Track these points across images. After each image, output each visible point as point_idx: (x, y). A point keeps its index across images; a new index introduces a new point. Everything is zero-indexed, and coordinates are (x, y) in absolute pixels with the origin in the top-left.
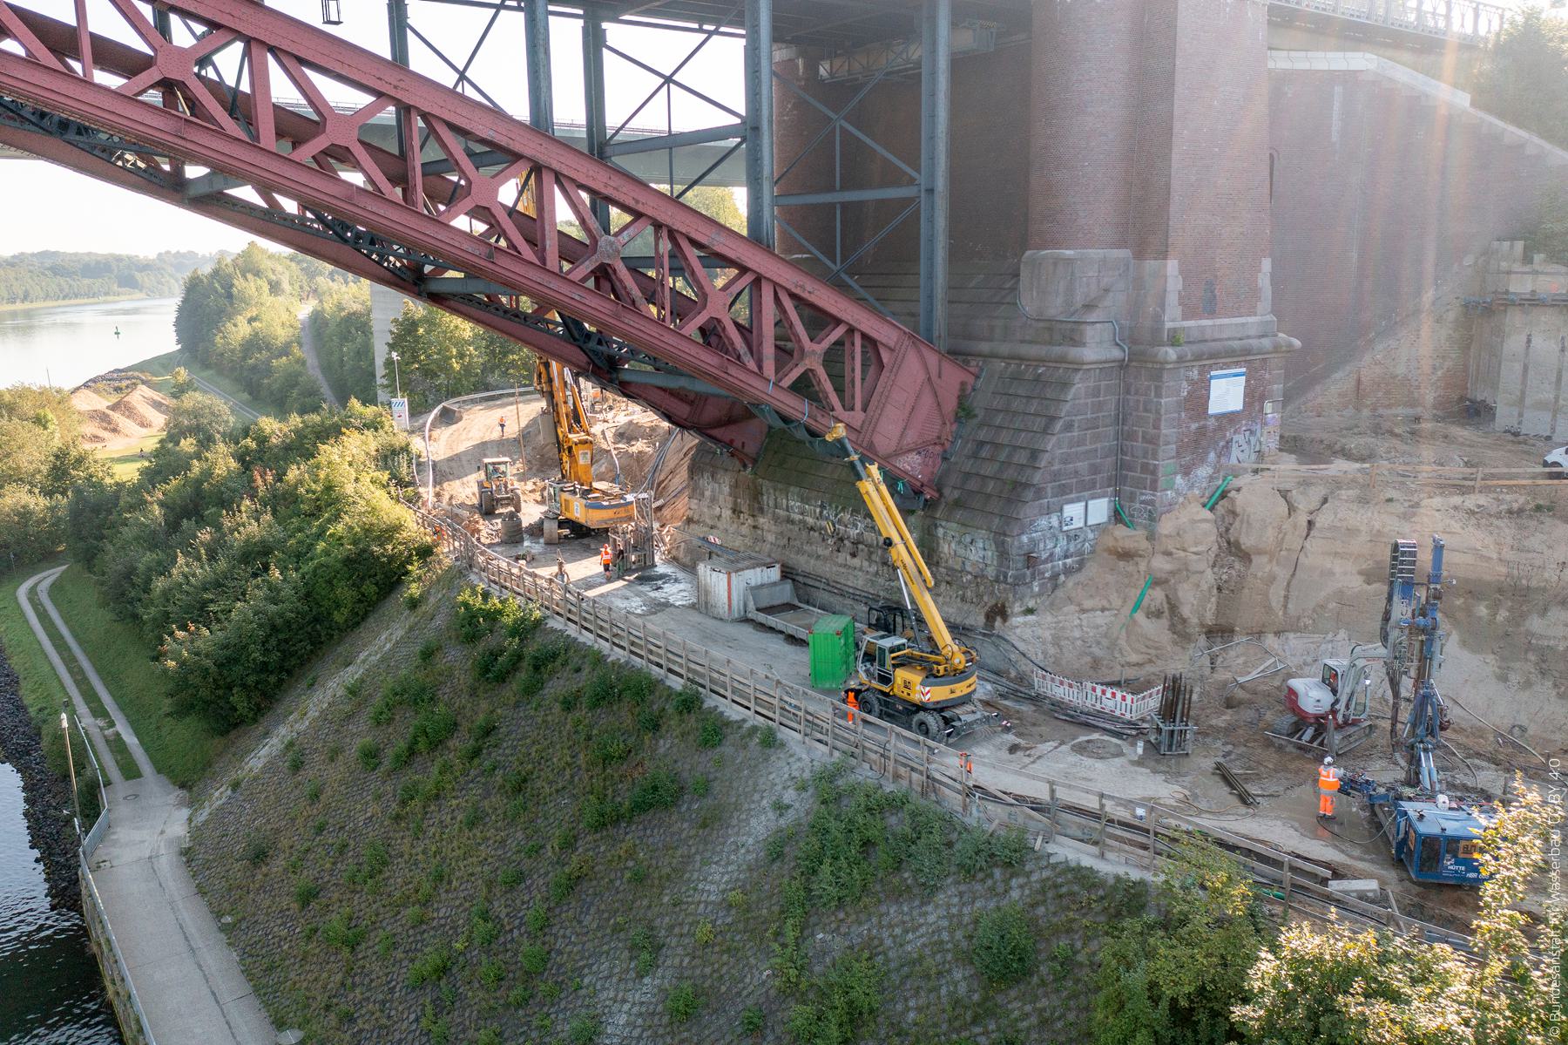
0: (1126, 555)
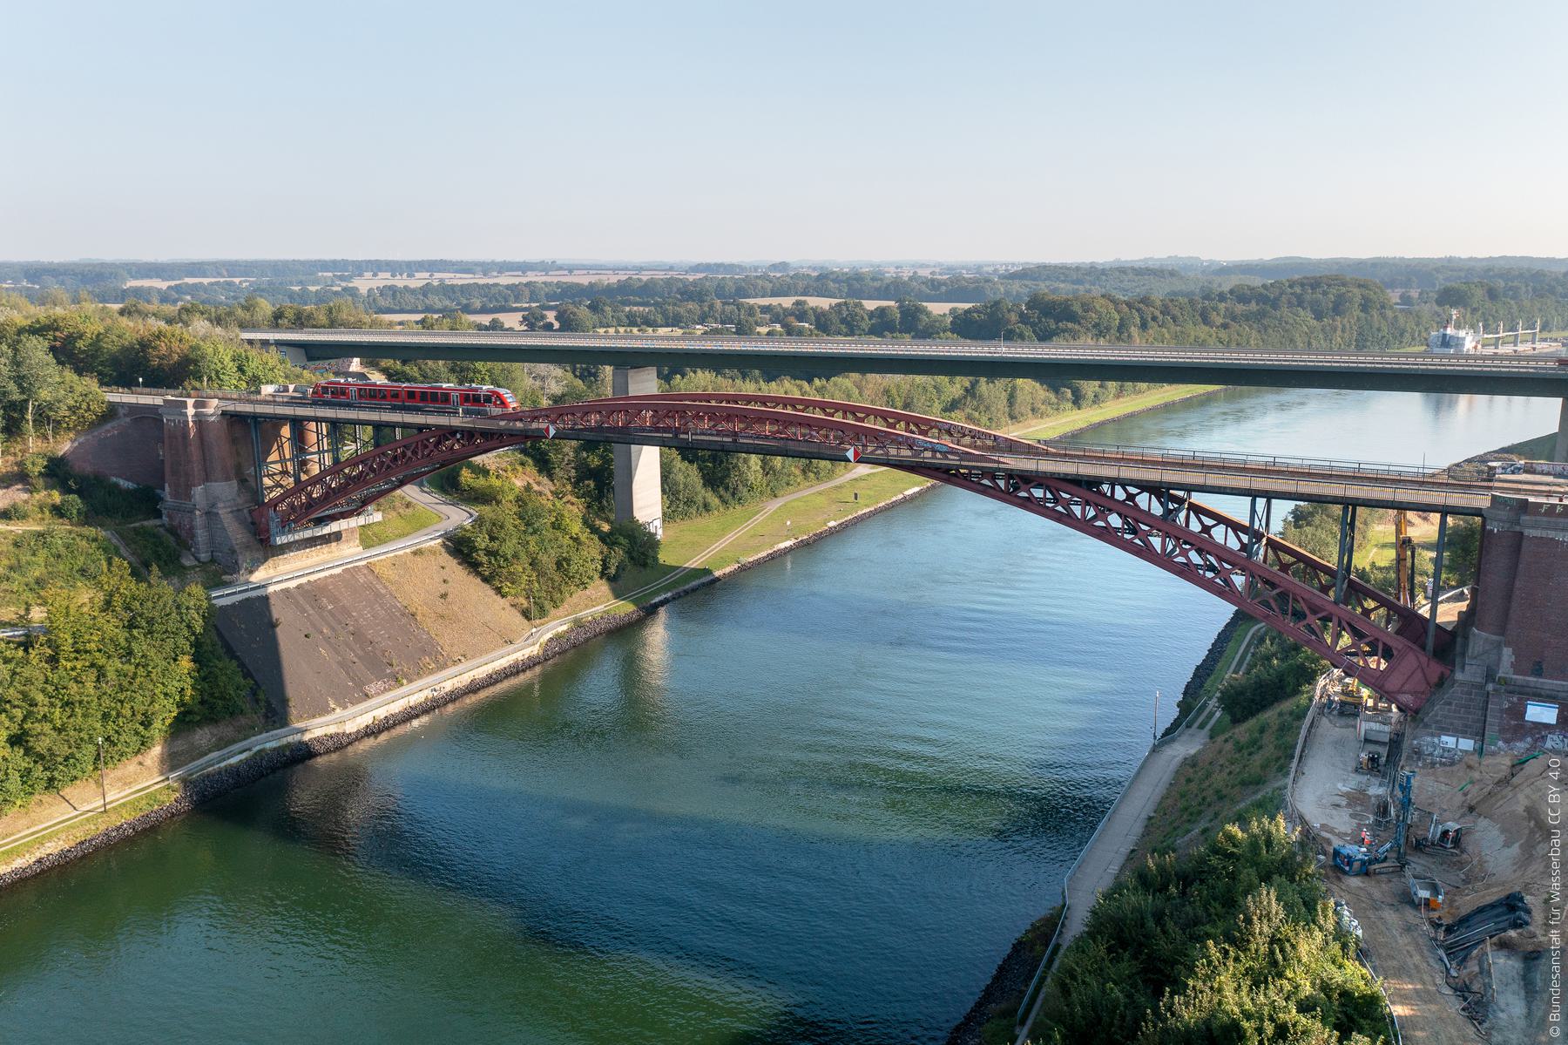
0: (1470, 767)
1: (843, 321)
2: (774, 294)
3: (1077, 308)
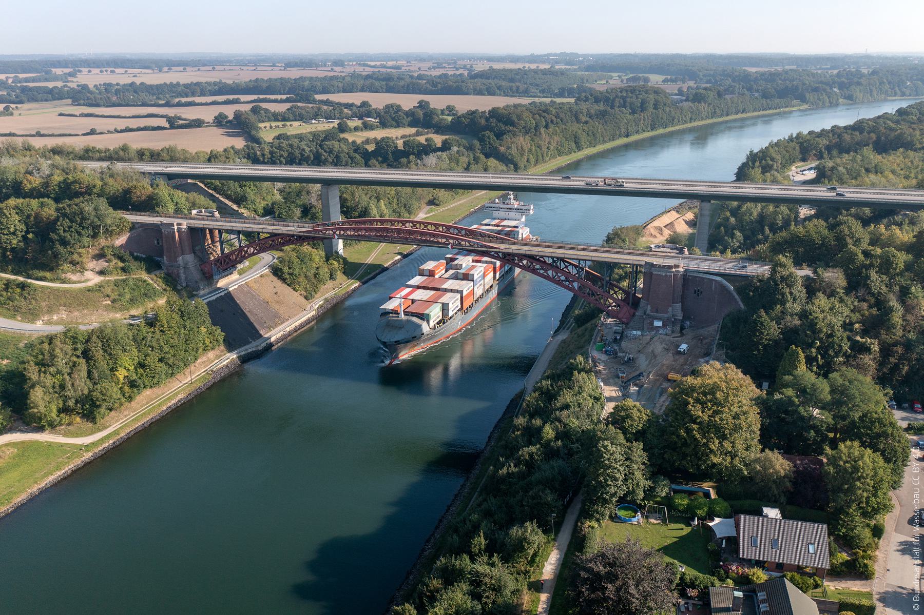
1: (393, 119)
2: (345, 91)
3: (514, 118)
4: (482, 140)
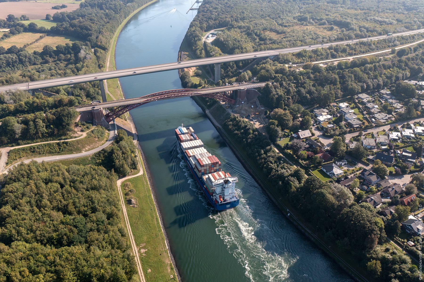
4: (90, 41)
